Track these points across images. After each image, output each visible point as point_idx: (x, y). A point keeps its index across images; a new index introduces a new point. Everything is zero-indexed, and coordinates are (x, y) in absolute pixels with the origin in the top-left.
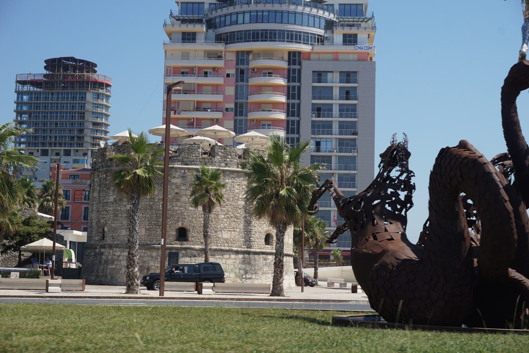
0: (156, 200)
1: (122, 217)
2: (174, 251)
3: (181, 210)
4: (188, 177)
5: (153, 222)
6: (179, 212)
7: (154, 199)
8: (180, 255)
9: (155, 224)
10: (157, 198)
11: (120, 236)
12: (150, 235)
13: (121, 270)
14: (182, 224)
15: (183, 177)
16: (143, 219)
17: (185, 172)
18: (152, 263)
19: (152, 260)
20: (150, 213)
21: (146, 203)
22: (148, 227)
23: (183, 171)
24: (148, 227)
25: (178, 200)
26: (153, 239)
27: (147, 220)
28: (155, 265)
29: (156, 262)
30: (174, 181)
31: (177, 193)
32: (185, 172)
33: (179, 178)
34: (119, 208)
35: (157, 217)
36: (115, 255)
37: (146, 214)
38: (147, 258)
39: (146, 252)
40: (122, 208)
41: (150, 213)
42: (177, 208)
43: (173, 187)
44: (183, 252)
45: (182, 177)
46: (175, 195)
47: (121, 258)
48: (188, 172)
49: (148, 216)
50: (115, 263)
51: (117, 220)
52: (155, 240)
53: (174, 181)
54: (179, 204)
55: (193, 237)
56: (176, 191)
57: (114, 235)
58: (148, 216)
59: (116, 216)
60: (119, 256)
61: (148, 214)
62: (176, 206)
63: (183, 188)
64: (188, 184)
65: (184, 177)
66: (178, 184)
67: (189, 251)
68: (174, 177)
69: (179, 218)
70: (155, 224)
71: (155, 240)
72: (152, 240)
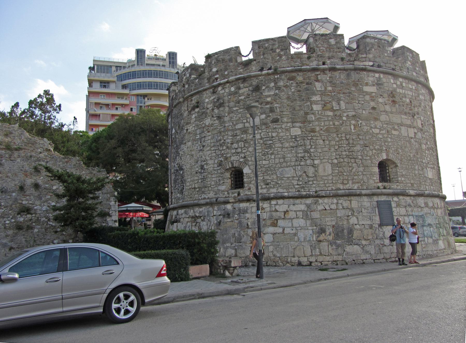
0: (344, 118)
1: (282, 148)
2: (383, 198)
3: (383, 134)
4: (385, 85)
5: (344, 153)
6: (381, 136)
7: (340, 117)
8: (393, 205)
9: (347, 156)
10: (345, 115)
11: (282, 179)
12: (341, 173)
13: (295, 234)
14: (387, 155)
15: (379, 84)
16: (326, 149)
17: (379, 77)
18: (353, 220)
19: (353, 215)
20: (337, 139)
21: (327, 123)
22: (335, 161)
23: (377, 75)
24: (335, 161)
25: (376, 119)
26: (348, 180)
27: (333, 149)
28: (360, 223)
29: (360, 217)
30: (367, 89)
31: (374, 108)
32: (379, 77)
33: (374, 85)
34: (274, 135)
35: (349, 144)
36: (276, 211)
37: (330, 141)
38: (343, 211)
39: (340, 202)
40: (282, 134)
41: (337, 139)
42: (377, 131)
43: (367, 98)
44: (395, 199)
45: (378, 84)
46: (371, 111)
47: (291, 215)
48: (384, 77)
49: (333, 143)
50: (281, 223)
51: (272, 154)
52: (350, 182)
53: (367, 89)
54: (379, 124)
55: (402, 176)
56: (372, 104)
57: (266, 177)
58: (333, 143)
59: (270, 147)
60: (286, 212)
61: (334, 139)
62: (376, 127)
63: (380, 100)
64: (385, 95)
65: (380, 84)
66: (374, 94)
67: (401, 197)
68: (367, 84)
69: (381, 146)
70: (347, 156)
71: (350, 182)
72: (345, 182)
